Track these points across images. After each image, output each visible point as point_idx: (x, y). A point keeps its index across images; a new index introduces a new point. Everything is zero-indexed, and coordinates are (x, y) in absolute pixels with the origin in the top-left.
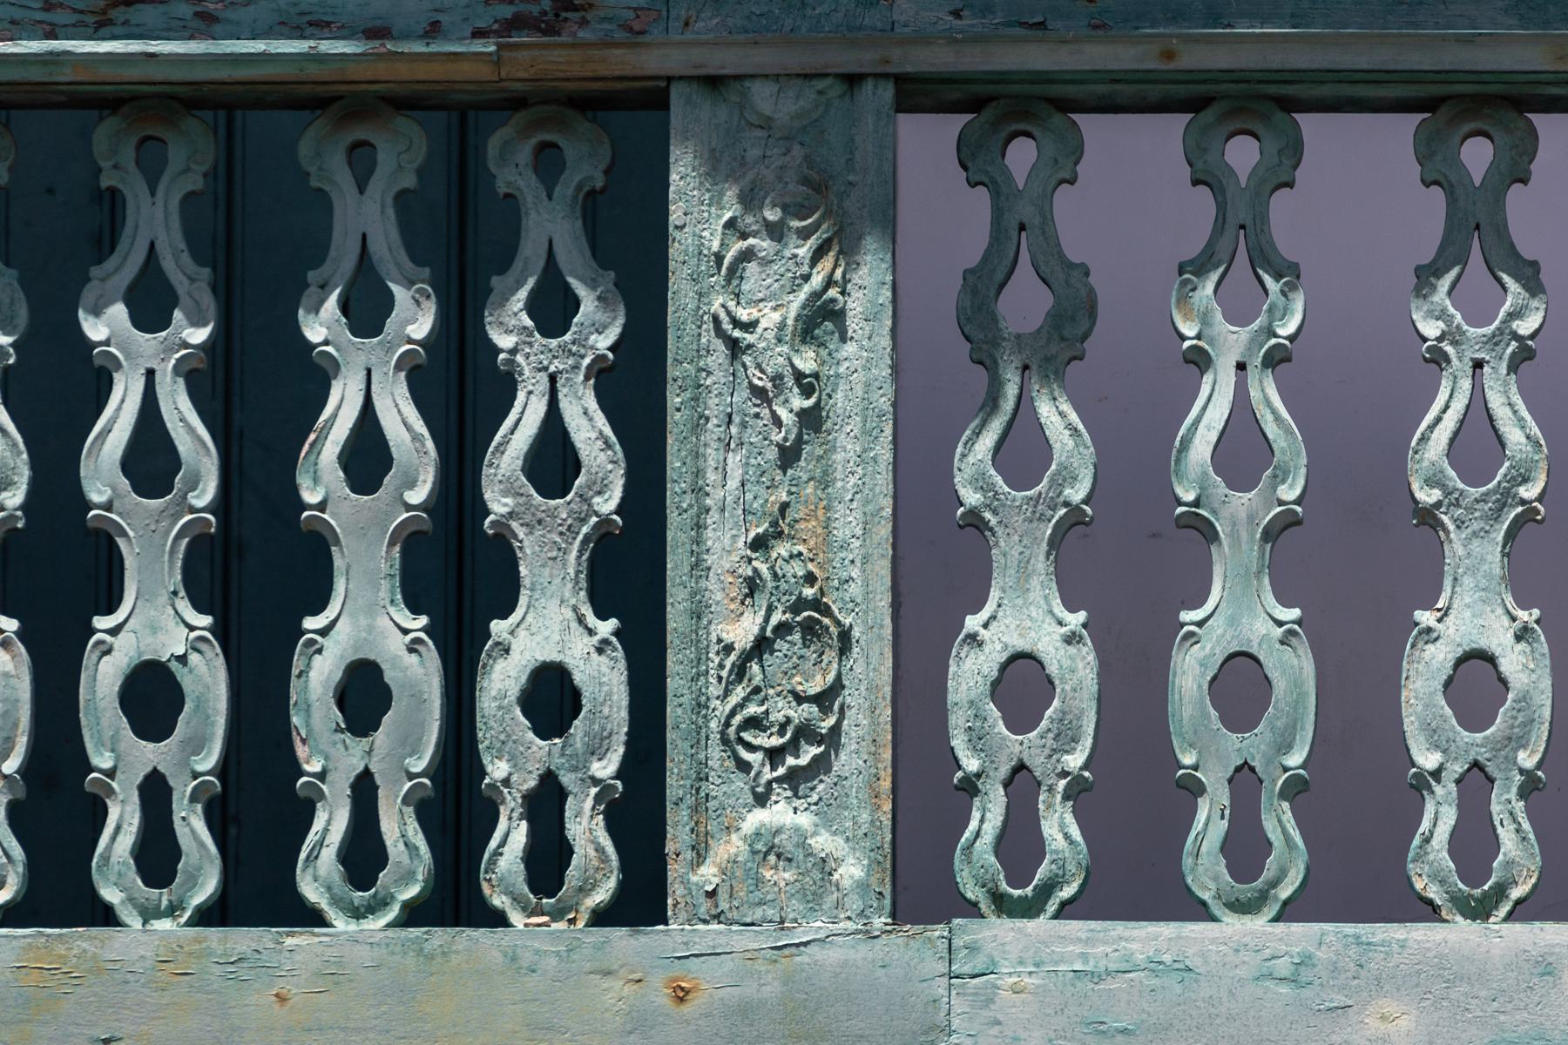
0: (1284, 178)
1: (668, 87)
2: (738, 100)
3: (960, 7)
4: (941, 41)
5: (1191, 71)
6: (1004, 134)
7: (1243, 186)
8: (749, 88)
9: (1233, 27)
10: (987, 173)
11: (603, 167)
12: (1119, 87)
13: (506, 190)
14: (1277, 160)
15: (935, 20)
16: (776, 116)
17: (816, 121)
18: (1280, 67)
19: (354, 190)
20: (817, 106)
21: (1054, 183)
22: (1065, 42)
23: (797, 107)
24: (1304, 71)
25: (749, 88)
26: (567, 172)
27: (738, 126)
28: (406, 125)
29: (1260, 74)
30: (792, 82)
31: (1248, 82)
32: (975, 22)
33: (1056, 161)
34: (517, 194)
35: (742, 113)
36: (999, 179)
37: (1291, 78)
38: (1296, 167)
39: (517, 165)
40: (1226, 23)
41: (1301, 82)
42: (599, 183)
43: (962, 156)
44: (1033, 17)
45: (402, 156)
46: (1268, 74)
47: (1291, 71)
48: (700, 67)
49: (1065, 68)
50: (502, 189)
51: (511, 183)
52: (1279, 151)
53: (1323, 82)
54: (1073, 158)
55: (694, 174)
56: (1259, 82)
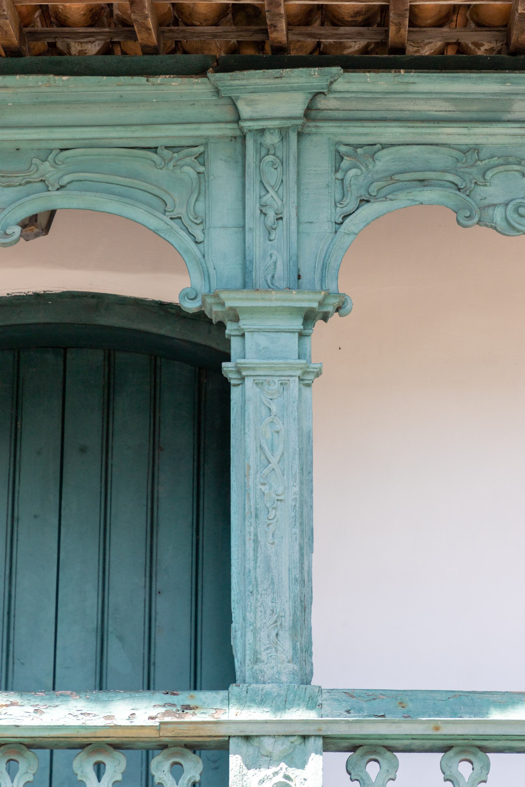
0: (483, 779)
1: (229, 739)
2: (258, 745)
3: (350, 709)
4: (343, 722)
5: (446, 735)
6: (366, 760)
7: (467, 782)
8: (263, 740)
9: (462, 717)
10: (359, 775)
11: (199, 772)
12: (415, 741)
13: (159, 781)
14: (480, 771)
15: (339, 714)
16: (274, 752)
17: (290, 754)
18: (483, 734)
19: (97, 780)
20: (290, 748)
21: (387, 779)
22: (394, 723)
23: (283, 748)
24: (493, 735)
25: (263, 740)
26: (184, 774)
27: (258, 756)
28: (118, 755)
29: (474, 736)
30: (281, 738)
31: (468, 739)
32: (355, 715)
33: (388, 771)
34: (163, 783)
35: (259, 750)
36: (364, 778)
37: (487, 738)
38: (487, 774)
39: (164, 771)
40: (459, 716)
41: (491, 740)
42: (198, 779)
43: (349, 769)
44: (379, 713)
45: (116, 767)
46: (478, 736)
47: (487, 735)
48: (243, 732)
49: (394, 733)
50: (157, 780)
51: (161, 778)
52: (481, 768)
53: (499, 740)
54: (395, 770)
55: (240, 775)
56: (473, 740)
